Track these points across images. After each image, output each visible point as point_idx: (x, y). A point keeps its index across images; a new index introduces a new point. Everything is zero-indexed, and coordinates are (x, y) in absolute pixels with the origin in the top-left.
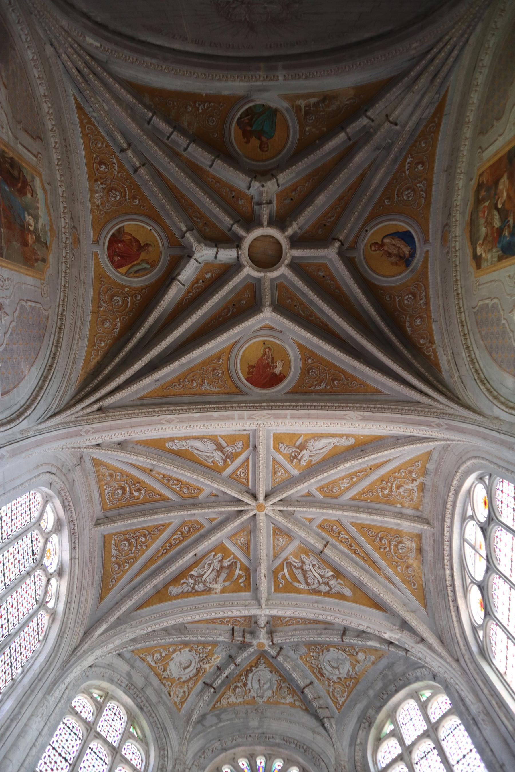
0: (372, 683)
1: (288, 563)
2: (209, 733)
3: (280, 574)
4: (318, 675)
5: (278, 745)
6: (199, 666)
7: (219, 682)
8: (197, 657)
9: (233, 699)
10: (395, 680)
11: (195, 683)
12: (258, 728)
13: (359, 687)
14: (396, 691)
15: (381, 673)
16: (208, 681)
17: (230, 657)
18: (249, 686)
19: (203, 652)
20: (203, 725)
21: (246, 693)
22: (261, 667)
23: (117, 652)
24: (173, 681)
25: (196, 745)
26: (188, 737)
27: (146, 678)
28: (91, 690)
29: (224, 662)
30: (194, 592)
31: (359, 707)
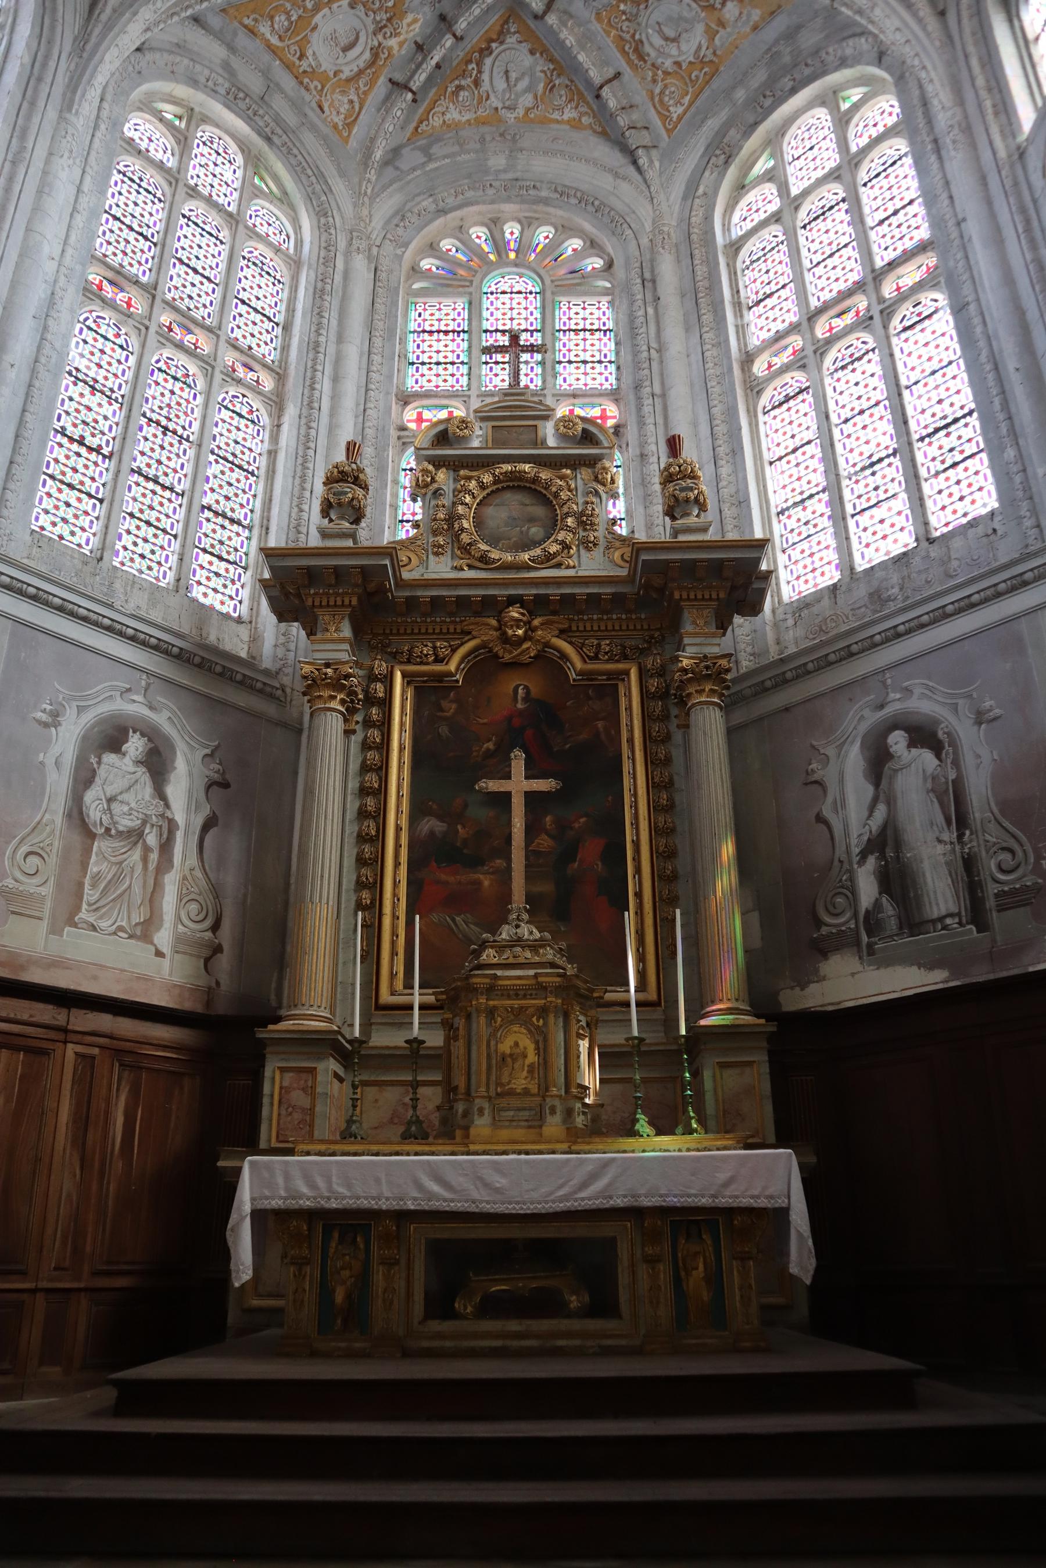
0: (745, 74)
2: (409, 182)
4: (633, 57)
5: (546, 202)
6: (376, 43)
7: (421, 78)
8: (369, 21)
9: (454, 115)
10: (796, 65)
11: (372, 83)
12: (505, 171)
13: (716, 83)
14: (794, 91)
15: (769, 49)
16: (398, 77)
17: (443, 18)
18: (486, 85)
19: (380, 8)
21: (480, 102)
22: (511, 40)
23: (189, 12)
24: (324, 79)
25: (387, 205)
26: (369, 191)
27: (266, 74)
28: (155, 105)
29: (429, 31)
31: (713, 124)
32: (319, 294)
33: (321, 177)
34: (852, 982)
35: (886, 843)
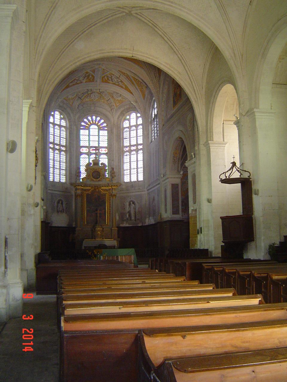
1: (107, 76)
18: (91, 97)
20: (79, 109)
30: (77, 84)
31: (122, 109)
32: (70, 133)
34: (125, 225)
35: (129, 212)
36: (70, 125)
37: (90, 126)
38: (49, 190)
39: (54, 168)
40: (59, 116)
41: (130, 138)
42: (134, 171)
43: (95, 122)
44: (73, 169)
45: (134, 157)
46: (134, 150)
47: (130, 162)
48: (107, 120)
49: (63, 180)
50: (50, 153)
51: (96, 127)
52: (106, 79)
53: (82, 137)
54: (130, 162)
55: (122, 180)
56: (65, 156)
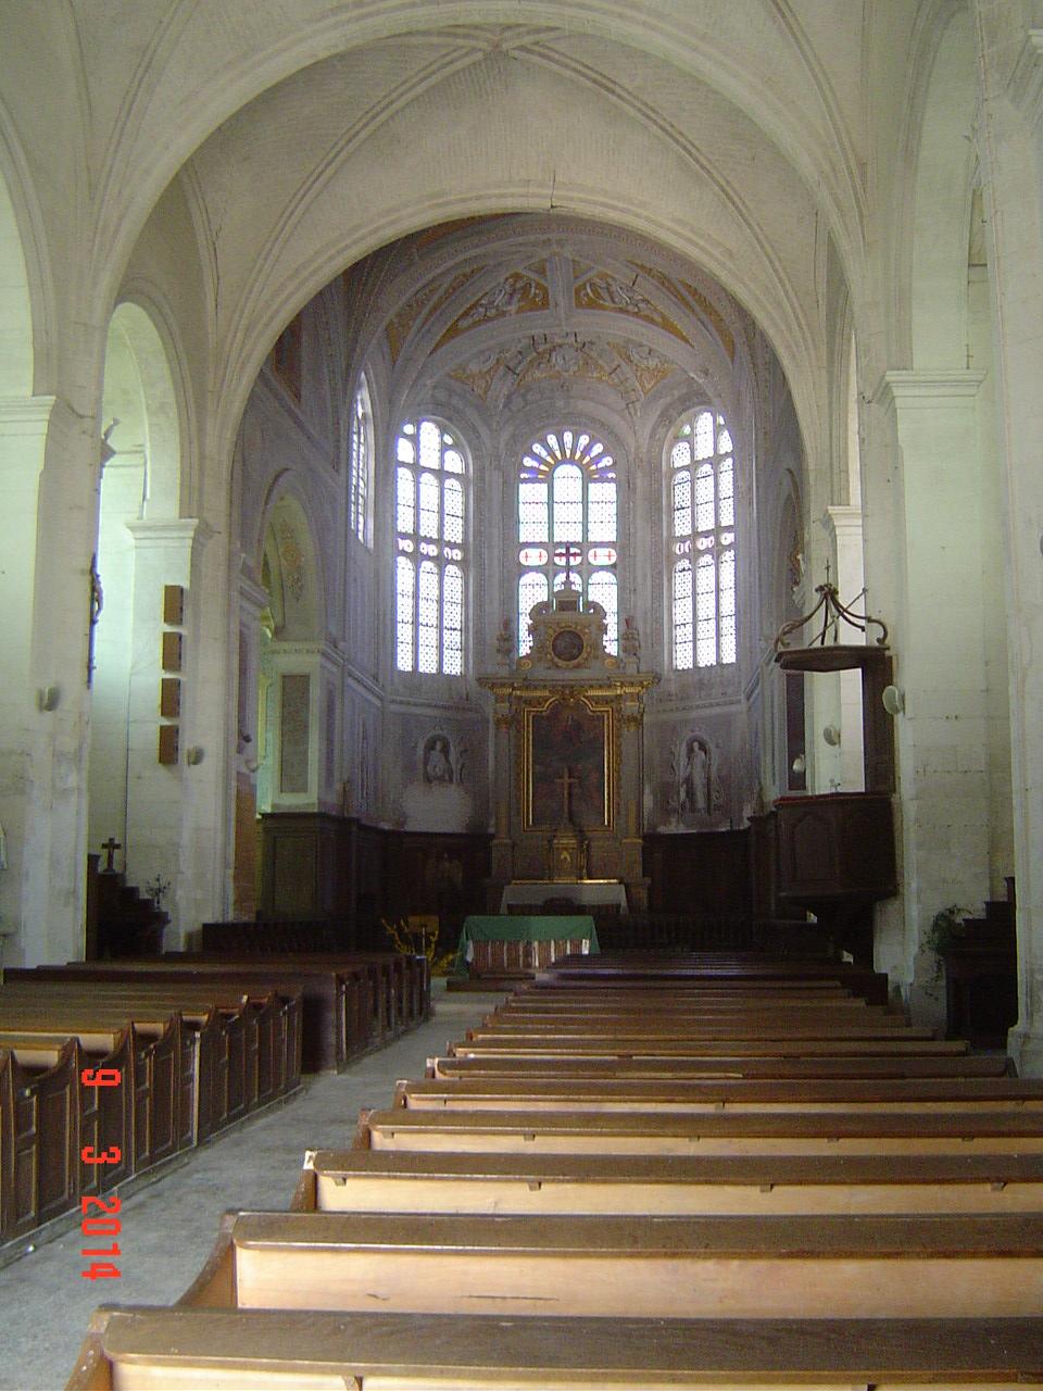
3: (583, 292)
20: (510, 410)
30: (487, 319)
33: (474, 429)
34: (675, 827)
35: (689, 781)
36: (480, 471)
37: (553, 468)
38: (393, 701)
39: (416, 623)
40: (438, 440)
41: (694, 505)
42: (707, 629)
43: (573, 453)
44: (488, 624)
45: (706, 578)
46: (708, 551)
47: (695, 594)
48: (614, 443)
49: (454, 665)
50: (399, 571)
51: (575, 471)
52: (591, 295)
53: (524, 512)
54: (695, 594)
55: (666, 662)
56: (459, 581)
